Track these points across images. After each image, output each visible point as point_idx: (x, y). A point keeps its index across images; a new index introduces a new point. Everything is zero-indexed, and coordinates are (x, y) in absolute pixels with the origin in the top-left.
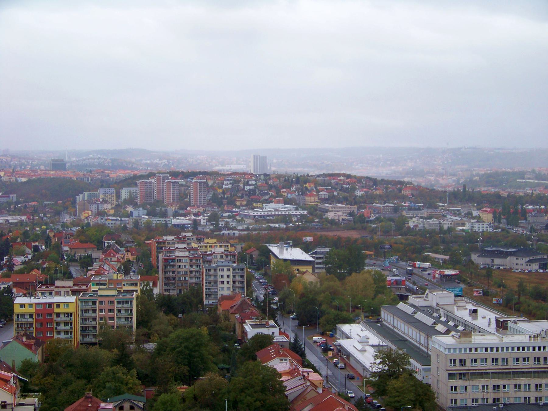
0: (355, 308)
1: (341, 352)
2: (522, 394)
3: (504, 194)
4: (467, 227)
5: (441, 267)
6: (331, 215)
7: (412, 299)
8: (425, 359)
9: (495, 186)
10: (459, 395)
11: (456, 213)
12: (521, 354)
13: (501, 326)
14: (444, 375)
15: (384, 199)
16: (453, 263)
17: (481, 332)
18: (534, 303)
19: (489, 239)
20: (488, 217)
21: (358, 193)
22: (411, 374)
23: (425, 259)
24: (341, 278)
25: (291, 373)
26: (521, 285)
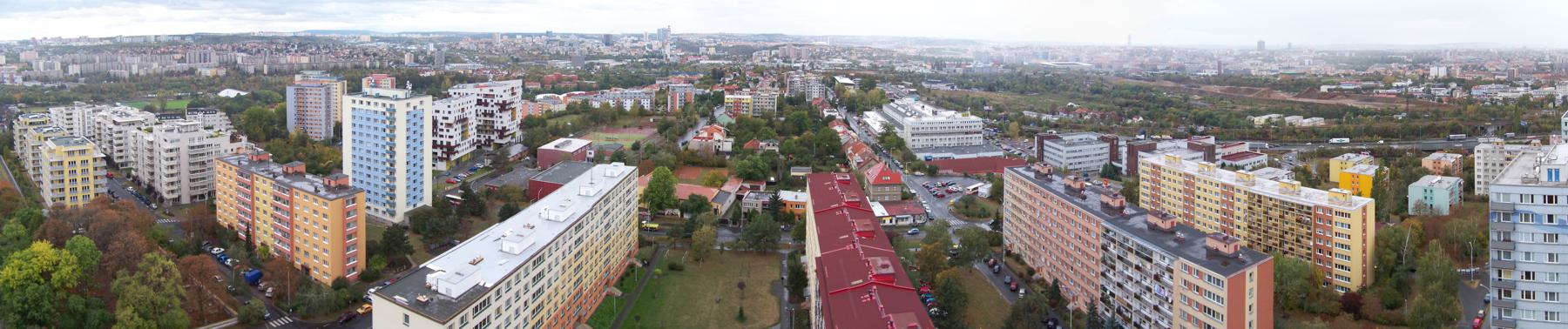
0: (872, 104)
1: (865, 124)
2: (943, 143)
3: (936, 57)
4: (920, 71)
5: (908, 87)
6: (862, 65)
7: (896, 101)
8: (902, 127)
9: (931, 53)
10: (916, 143)
11: (916, 65)
12: (943, 125)
13: (935, 113)
14: (909, 135)
15: (885, 58)
16: (914, 86)
17: (926, 116)
18: (948, 103)
19: (930, 76)
20: (929, 67)
21: (874, 55)
22: (895, 134)
23: (902, 84)
24: (866, 91)
25: (843, 132)
26: (943, 97)
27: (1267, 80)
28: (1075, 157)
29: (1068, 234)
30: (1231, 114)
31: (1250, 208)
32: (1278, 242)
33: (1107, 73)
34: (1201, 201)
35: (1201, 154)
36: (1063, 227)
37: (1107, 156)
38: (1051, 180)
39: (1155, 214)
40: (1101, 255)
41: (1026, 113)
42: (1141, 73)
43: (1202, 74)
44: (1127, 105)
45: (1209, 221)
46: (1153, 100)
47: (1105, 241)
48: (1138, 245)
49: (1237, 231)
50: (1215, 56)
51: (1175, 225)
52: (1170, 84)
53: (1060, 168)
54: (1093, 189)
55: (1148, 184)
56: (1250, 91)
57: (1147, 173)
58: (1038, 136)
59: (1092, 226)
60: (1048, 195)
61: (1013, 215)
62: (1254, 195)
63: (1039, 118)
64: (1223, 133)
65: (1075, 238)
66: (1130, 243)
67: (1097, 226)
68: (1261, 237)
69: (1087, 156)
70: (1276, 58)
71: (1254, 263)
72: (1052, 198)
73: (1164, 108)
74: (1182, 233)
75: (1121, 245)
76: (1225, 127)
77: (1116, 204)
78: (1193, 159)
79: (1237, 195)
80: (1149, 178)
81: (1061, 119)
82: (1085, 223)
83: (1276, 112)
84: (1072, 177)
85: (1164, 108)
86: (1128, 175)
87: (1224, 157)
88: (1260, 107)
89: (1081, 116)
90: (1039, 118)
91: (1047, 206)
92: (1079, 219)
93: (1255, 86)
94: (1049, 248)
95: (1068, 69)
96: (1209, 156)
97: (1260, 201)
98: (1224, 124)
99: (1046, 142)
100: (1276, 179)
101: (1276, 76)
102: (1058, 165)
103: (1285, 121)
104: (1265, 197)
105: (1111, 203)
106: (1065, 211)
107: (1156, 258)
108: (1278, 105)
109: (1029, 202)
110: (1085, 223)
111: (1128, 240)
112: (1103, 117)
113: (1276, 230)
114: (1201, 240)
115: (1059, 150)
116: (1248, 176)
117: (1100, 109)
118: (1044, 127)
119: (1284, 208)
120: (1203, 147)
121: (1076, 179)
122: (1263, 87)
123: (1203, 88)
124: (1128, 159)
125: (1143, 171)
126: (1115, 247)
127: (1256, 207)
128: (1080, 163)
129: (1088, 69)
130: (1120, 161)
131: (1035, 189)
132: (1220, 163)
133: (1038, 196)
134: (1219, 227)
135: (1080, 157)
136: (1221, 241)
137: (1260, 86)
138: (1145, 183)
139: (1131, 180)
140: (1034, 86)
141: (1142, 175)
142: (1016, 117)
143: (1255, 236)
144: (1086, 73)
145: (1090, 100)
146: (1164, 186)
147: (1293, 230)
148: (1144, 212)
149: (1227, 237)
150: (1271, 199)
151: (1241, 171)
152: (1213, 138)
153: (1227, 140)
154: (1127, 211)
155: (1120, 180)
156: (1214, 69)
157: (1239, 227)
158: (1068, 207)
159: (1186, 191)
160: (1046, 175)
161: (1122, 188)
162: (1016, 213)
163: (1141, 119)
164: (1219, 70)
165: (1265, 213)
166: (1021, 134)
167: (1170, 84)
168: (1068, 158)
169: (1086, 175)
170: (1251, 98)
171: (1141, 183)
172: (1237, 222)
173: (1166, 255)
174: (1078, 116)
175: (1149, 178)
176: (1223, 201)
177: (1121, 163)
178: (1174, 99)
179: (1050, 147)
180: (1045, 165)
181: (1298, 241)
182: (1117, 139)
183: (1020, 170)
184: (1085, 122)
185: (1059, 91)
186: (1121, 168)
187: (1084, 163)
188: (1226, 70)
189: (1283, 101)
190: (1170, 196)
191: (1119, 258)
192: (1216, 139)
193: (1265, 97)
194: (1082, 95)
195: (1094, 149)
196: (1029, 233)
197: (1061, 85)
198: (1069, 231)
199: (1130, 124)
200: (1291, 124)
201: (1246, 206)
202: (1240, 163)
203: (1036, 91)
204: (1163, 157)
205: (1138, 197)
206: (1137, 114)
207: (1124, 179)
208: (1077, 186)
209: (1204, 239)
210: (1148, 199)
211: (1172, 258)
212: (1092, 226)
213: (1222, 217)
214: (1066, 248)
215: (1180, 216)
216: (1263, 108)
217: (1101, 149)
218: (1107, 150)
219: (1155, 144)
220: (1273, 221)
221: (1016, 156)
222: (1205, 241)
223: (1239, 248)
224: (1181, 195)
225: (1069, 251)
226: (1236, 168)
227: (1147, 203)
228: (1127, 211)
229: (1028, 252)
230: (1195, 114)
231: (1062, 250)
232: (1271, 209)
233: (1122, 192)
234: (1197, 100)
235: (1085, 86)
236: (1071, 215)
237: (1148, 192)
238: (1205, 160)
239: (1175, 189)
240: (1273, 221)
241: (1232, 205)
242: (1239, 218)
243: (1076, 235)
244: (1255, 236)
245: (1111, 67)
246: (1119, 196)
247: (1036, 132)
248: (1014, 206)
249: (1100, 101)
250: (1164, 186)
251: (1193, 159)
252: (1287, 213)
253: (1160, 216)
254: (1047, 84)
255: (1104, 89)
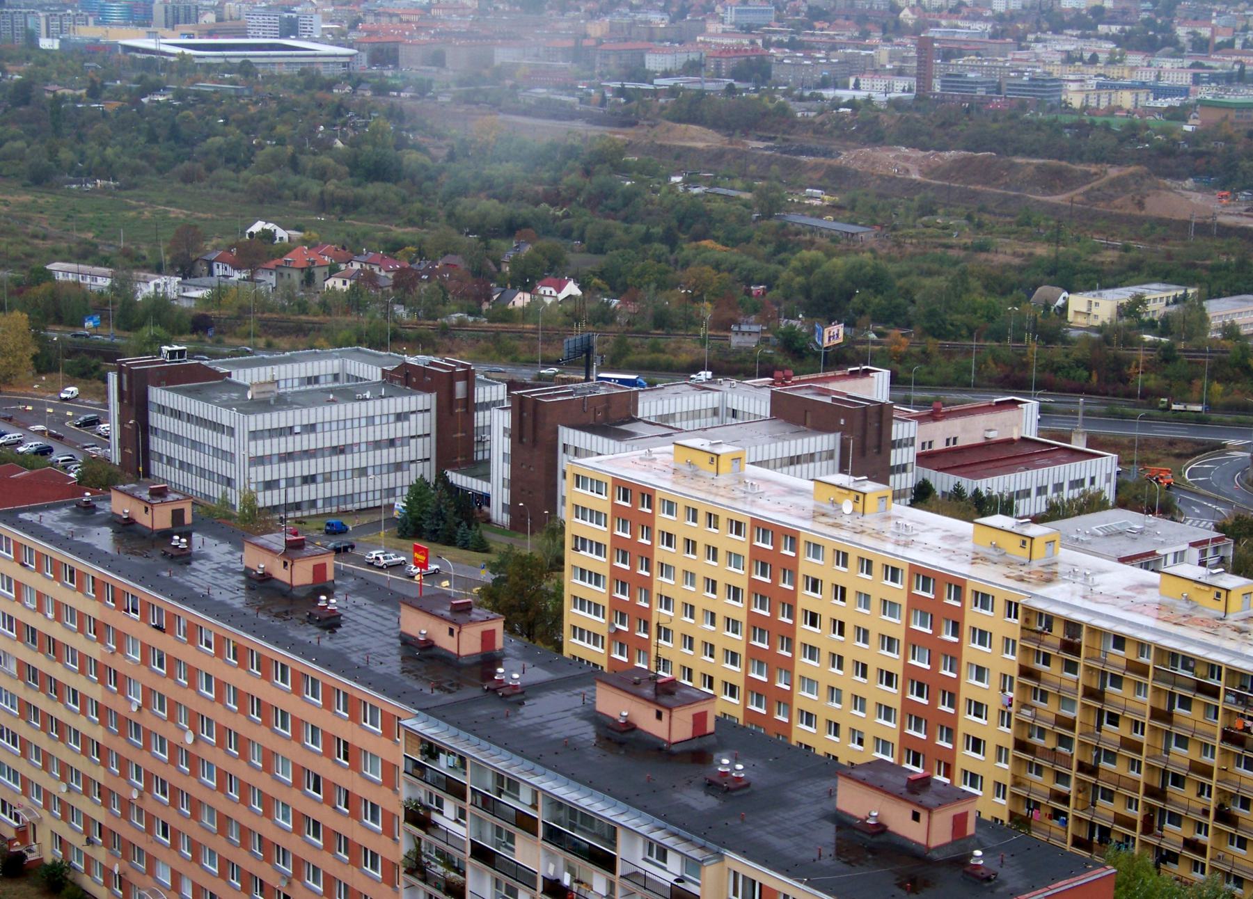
27: (1133, 132)
28: (287, 457)
29: (268, 768)
30: (964, 273)
31: (1026, 672)
32: (1138, 815)
33: (423, 89)
34: (821, 636)
35: (827, 442)
36: (243, 744)
37: (426, 448)
38: (184, 558)
39: (626, 681)
40: (405, 846)
41: (62, 271)
42: (571, 89)
43: (846, 95)
44: (511, 228)
45: (852, 717)
46: (626, 207)
47: (422, 793)
48: (558, 804)
49: (966, 758)
50: (907, 16)
51: (710, 727)
52: (701, 138)
53: (225, 502)
54: (368, 588)
55: (599, 563)
56: (1055, 179)
57: (597, 516)
58: (120, 371)
59: (367, 736)
60: (174, 618)
61: (27, 710)
62: (1049, 620)
63: (122, 288)
64: (925, 357)
65: (297, 783)
66: (525, 795)
67: (388, 733)
68: (1071, 789)
69: (339, 450)
70: (1181, 32)
71: (1033, 888)
72: (193, 632)
73: (670, 240)
74: (736, 759)
75: (488, 804)
76: (937, 331)
77: (468, 643)
78: (794, 460)
79: (975, 616)
80: (606, 540)
81: (219, 294)
82: (338, 724)
83: (1164, 276)
84: (277, 540)
85: (670, 240)
86: (519, 522)
87: (926, 458)
88: (1095, 250)
89: (309, 279)
90: (122, 288)
91: (174, 662)
92: (309, 708)
93: (1080, 158)
94: (191, 829)
95: (246, 69)
96: (862, 450)
97: (1071, 647)
98: (932, 314)
99: (158, 395)
100: (1148, 560)
101: (1177, 114)
102: (215, 491)
103: (1204, 319)
104: (1093, 630)
105: (445, 641)
106: (250, 681)
107: (630, 854)
108: (1176, 247)
109: (95, 651)
110: (338, 724)
111: (514, 786)
112: (405, 282)
113: (1135, 765)
114: (819, 786)
115: (216, 427)
116: (1027, 541)
117: (394, 247)
118: (149, 331)
119: (1174, 680)
120: (847, 414)
121: (294, 548)
122: (1115, 162)
123: (845, 158)
124: (515, 458)
125: (580, 511)
126: (462, 814)
127: (1053, 671)
128: (309, 480)
129: (340, 70)
130: (481, 469)
131: (118, 596)
132: (906, 481)
133: (130, 623)
134: (894, 738)
135: (308, 454)
136: (899, 797)
137: (1099, 158)
138: (588, 559)
139: (529, 546)
140: (91, 148)
141: (575, 526)
142: (19, 288)
143: (1042, 784)
144: (329, 85)
145: (350, 206)
146: (666, 569)
147: (1207, 771)
148: (588, 674)
149: (925, 782)
150: (1120, 641)
151: (998, 520)
152: (885, 374)
153: (946, 384)
154: (510, 673)
155: (482, 547)
156: (900, 73)
157: (977, 745)
158: (264, 665)
159: (760, 594)
160: (166, 535)
161: (486, 576)
162: (40, 701)
163: (572, 289)
164: (924, 77)
165: (1089, 693)
166: (45, 364)
167: (701, 138)
168: (259, 461)
169: (336, 530)
170: (1055, 209)
171: (572, 558)
172: (968, 723)
173: (669, 841)
174: (297, 277)
175: (606, 540)
176: (915, 642)
177: (486, 477)
178: (718, 205)
179: (177, 414)
180: (160, 493)
181: (1224, 816)
182: (468, 376)
183: (50, 519)
184: (325, 307)
185: (210, 169)
186: (485, 499)
187: (327, 478)
188: (951, 81)
189: (1204, 229)
190: (690, 610)
191: (480, 853)
192: (894, 380)
193: (1123, 205)
194: (315, 188)
195: (370, 420)
196: (99, 775)
197: (219, 140)
198: (269, 757)
199: (526, 312)
200: (1230, 331)
201: (1011, 662)
202: (996, 484)
203: (106, 170)
204: (664, 452)
205: (559, 615)
206: (554, 270)
207: (499, 543)
208: (301, 574)
209: (827, 784)
210: (598, 623)
211: (696, 854)
212: (367, 736)
213: (906, 702)
214: (264, 828)
215: (732, 690)
216: (1109, 256)
217: (401, 417)
218: (424, 423)
219: (632, 401)
220: (1124, 730)
221: (23, 461)
222: (832, 794)
223: (971, 829)
224: (738, 609)
225: (271, 834)
226: (980, 506)
227: (595, 638)
228: (510, 673)
229: (101, 854)
230: (808, 269)
231: (245, 832)
232: (1117, 681)
233: (491, 596)
234: (819, 212)
235: (324, 145)
236: (277, 693)
237: (600, 593)
238: (843, 469)
239: (712, 585)
240: (1124, 730)
241: (953, 657)
242: (978, 709)
243: (299, 771)
244: (1042, 784)
245: (438, 60)
246: (477, 613)
247: (111, 355)
248: (29, 673)
249: (391, 213)
250: (666, 569)
251: (794, 460)
252: (1186, 703)
253: (648, 691)
254: (153, 138)
255: (411, 158)
